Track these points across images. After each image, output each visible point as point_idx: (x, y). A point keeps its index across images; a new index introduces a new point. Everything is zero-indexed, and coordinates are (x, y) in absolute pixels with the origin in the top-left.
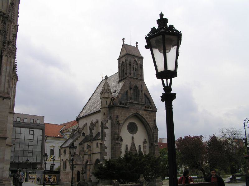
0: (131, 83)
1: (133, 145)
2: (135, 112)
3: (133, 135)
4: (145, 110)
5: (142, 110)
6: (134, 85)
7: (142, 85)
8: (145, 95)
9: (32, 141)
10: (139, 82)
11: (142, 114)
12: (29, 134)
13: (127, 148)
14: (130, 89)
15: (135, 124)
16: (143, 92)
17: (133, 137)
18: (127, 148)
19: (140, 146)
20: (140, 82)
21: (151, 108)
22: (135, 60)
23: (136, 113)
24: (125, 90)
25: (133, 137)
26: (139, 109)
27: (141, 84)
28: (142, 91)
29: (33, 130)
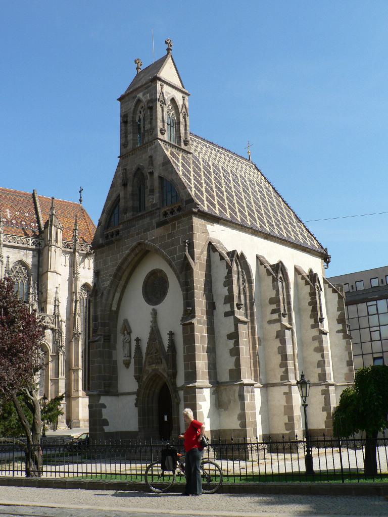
0: (126, 169)
1: (155, 333)
2: (135, 243)
3: (156, 307)
4: (159, 225)
5: (153, 229)
6: (135, 167)
7: (151, 157)
8: (160, 178)
9: (378, 328)
10: (144, 156)
11: (153, 241)
12: (369, 315)
13: (138, 348)
14: (125, 185)
15: (161, 271)
16: (156, 175)
17: (155, 313)
18: (138, 348)
19: (171, 334)
20: (147, 152)
21: (179, 209)
22: (139, 101)
23: (139, 244)
24: (114, 196)
25: (155, 313)
26: (144, 232)
27: (149, 153)
28: (151, 173)
29: (374, 303)
